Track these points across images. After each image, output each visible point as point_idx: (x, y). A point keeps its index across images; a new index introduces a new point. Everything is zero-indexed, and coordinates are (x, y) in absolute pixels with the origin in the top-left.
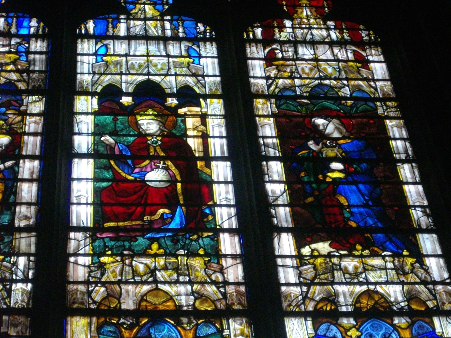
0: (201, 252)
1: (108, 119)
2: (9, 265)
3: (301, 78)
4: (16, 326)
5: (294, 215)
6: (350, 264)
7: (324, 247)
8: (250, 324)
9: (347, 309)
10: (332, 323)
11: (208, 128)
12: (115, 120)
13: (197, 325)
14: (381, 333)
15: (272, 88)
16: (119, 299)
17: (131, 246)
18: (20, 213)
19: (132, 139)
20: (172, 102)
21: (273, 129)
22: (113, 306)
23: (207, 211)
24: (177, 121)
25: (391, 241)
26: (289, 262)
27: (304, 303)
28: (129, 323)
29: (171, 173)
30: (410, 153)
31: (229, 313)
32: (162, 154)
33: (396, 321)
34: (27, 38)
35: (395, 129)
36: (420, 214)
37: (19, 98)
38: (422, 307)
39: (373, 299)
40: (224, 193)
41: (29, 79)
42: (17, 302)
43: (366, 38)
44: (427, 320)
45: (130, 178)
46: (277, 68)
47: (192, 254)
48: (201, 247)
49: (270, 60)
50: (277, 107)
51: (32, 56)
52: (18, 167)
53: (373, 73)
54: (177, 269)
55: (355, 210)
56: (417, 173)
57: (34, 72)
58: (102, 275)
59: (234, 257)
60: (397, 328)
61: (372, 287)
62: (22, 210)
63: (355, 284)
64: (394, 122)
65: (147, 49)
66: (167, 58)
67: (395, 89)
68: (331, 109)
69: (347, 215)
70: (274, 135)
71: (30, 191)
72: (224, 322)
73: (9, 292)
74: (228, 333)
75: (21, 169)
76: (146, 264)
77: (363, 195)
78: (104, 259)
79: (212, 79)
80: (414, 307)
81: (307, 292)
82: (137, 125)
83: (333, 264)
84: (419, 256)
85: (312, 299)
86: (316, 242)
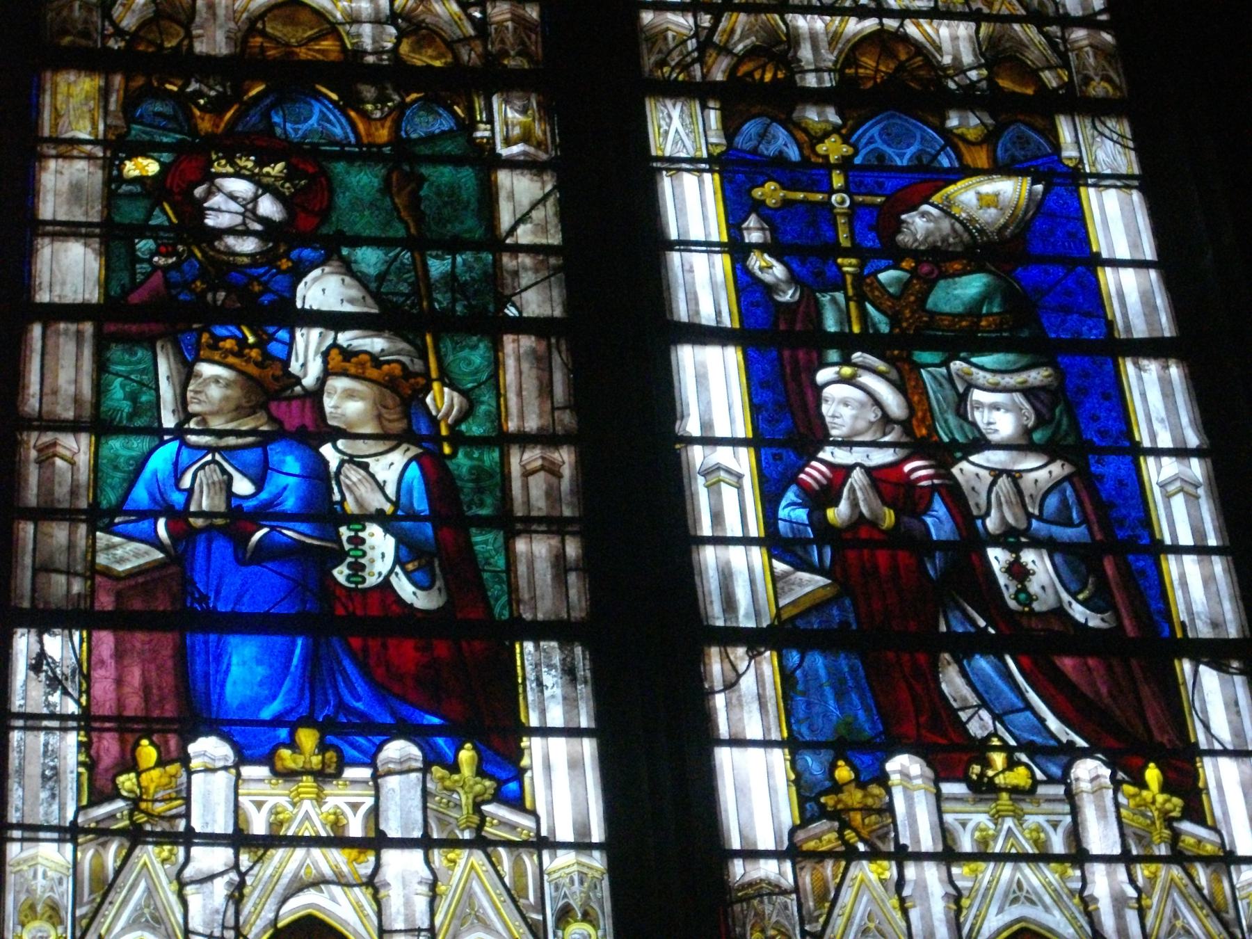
8: (546, 112)
9: (820, 80)
13: (402, 107)
27: (701, 60)
28: (213, 93)
31: (493, 78)
38: (1026, 85)
39: (894, 56)
44: (1039, 122)
60: (956, 140)
72: (478, 104)
74: (487, 134)
80: (1005, 83)
81: (713, 29)
85: (725, 50)
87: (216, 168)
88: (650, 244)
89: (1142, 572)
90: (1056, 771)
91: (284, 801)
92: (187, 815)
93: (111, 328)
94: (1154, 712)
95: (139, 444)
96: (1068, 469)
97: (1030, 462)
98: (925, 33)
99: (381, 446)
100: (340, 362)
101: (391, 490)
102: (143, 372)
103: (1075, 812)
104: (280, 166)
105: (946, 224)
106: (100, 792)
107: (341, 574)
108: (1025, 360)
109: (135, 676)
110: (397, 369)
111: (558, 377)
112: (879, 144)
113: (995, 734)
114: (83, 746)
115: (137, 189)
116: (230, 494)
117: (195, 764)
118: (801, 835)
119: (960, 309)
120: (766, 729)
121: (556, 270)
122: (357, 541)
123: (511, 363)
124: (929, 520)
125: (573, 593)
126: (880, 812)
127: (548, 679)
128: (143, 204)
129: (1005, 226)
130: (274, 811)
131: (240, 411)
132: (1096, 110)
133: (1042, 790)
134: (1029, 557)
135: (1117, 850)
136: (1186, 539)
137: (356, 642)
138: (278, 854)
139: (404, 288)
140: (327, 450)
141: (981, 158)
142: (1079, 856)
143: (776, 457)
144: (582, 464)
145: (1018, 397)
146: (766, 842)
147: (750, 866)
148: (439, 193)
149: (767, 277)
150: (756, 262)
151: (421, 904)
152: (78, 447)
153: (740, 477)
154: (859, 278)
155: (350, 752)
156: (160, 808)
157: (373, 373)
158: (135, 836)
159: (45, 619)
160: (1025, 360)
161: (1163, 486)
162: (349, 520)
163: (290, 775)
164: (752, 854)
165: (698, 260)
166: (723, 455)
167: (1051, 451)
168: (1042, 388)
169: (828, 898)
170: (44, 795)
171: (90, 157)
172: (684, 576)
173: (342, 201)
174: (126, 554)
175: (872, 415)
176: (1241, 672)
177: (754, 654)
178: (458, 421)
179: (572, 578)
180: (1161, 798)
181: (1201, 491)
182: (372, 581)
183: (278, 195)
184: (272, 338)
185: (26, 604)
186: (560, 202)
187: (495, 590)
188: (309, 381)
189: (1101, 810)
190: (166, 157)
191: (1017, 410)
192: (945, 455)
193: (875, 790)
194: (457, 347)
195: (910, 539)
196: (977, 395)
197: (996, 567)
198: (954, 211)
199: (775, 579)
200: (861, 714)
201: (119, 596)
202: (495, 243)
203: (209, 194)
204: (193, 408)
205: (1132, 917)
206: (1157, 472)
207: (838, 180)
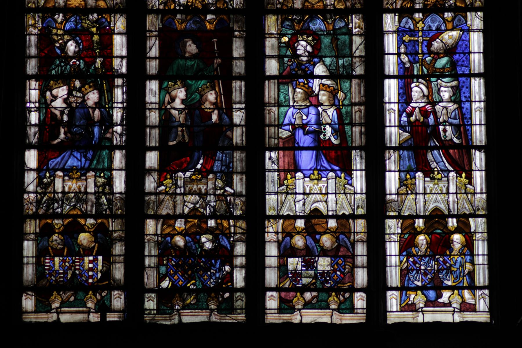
4: (237, 22)
9: (419, 6)
13: (335, 20)
14: (436, 25)
22: (289, 6)
33: (446, 15)
38: (462, 4)
44: (464, 14)
72: (350, 17)
80: (458, 4)
87: (299, 39)
89: (468, 130)
90: (446, 175)
91: (312, 185)
92: (296, 188)
93: (280, 81)
94: (466, 162)
95: (286, 108)
96: (457, 106)
97: (450, 104)
99: (329, 107)
100: (322, 86)
101: (331, 117)
102: (286, 91)
103: (448, 184)
104: (311, 37)
105: (441, 44)
106: (281, 185)
107: (322, 136)
108: (453, 79)
109: (286, 161)
110: (332, 88)
111: (362, 89)
113: (436, 167)
114: (278, 175)
115: (284, 45)
116: (302, 119)
117: (297, 178)
118: (399, 190)
119: (441, 67)
120: (395, 168)
121: (364, 62)
122: (325, 129)
123: (353, 86)
124: (429, 119)
125: (363, 139)
126: (414, 184)
127: (357, 159)
128: (285, 49)
130: (310, 187)
131: (304, 100)
132: (476, 10)
133: (443, 179)
134: (447, 127)
135: (455, 192)
136: (478, 123)
137: (324, 151)
138: (311, 196)
139: (334, 68)
140: (319, 108)
141: (450, 26)
142: (448, 193)
143: (402, 106)
144: (366, 110)
145: (450, 89)
146: (393, 192)
147: (390, 196)
148: (341, 43)
149: (404, 61)
150: (402, 56)
151: (334, 205)
152: (275, 109)
153: (395, 111)
154: (422, 59)
155: (323, 175)
156: (291, 187)
157: (328, 89)
158: (287, 193)
159: (271, 149)
160: (453, 79)
161: (475, 109)
162: (323, 124)
163: (312, 180)
164: (390, 194)
166: (392, 106)
167: (454, 102)
168: (455, 86)
169: (403, 202)
170: (272, 185)
171: (275, 37)
172: (383, 133)
173: (323, 46)
174: (284, 134)
175: (421, 95)
176: (484, 152)
177: (394, 152)
178: (343, 100)
179: (363, 136)
180: (464, 180)
181: (482, 110)
182: (327, 138)
183: (311, 45)
184: (310, 82)
185: (267, 146)
186: (365, 44)
187: (349, 139)
188: (316, 92)
189: (453, 183)
190: (289, 36)
191: (449, 92)
192: (433, 104)
193: (413, 180)
194: (344, 82)
195: (425, 124)
196: (442, 89)
197: (441, 130)
198: (443, 41)
199: (399, 134)
200: (412, 164)
201: (284, 143)
202: (352, 56)
203: (298, 45)
204: (296, 99)
205: (456, 205)
206: (475, 105)
207: (420, 34)
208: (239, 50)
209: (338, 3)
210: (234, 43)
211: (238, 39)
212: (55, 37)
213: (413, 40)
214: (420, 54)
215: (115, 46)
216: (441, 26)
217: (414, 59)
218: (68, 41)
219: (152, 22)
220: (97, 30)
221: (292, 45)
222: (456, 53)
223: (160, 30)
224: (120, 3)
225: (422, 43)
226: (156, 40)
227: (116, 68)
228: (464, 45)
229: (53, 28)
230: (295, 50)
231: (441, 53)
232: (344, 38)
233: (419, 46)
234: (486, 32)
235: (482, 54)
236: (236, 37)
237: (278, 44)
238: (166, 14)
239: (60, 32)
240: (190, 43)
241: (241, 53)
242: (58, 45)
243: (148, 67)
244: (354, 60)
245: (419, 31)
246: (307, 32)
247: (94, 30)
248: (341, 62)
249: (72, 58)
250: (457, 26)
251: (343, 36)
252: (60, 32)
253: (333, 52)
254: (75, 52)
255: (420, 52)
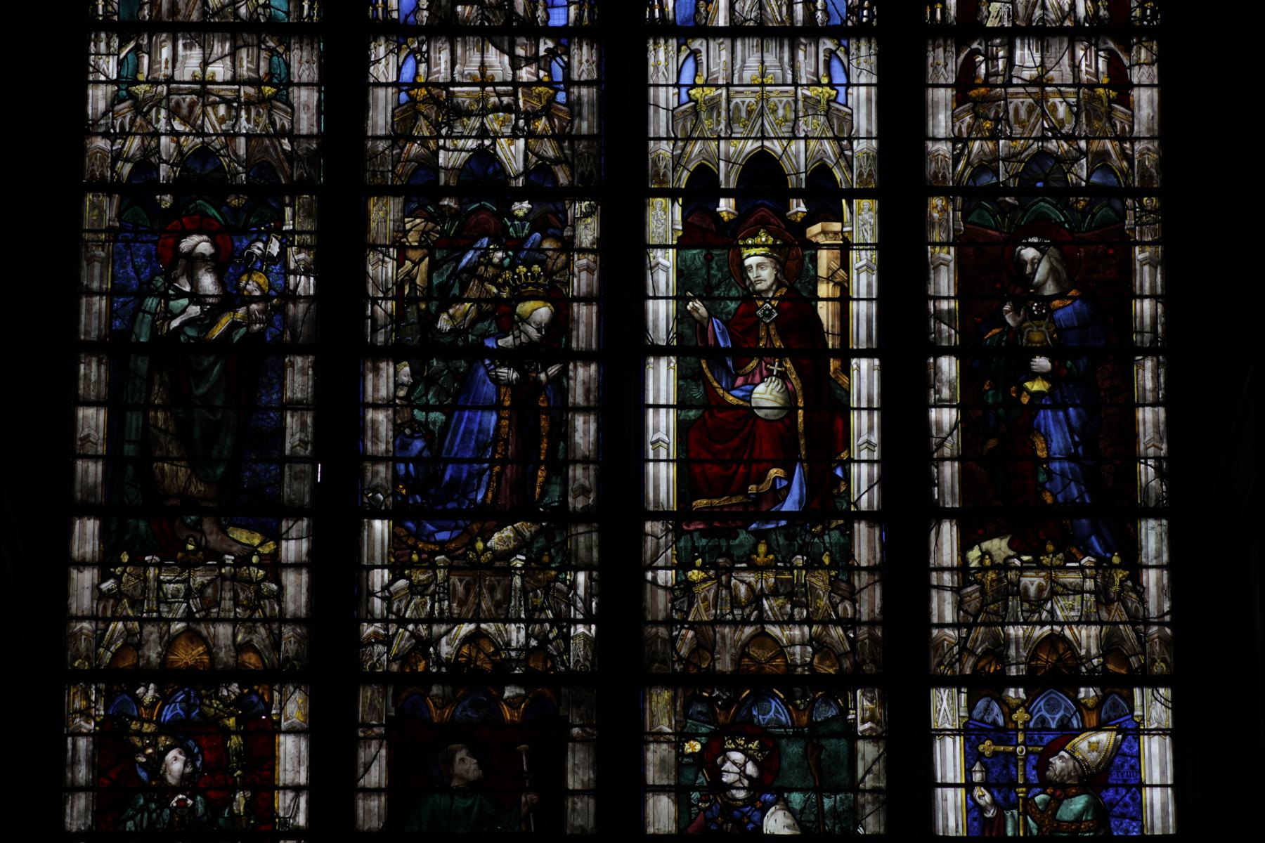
0: (826, 560)
1: (696, 254)
2: (565, 588)
3: (1010, 138)
5: (965, 476)
6: (1032, 582)
7: (998, 547)
8: (883, 701)
9: (1018, 670)
10: (993, 698)
11: (851, 288)
12: (708, 259)
13: (814, 701)
14: (1058, 716)
15: (960, 167)
16: (712, 652)
17: (729, 546)
18: (575, 479)
19: (733, 305)
20: (798, 208)
21: (952, 276)
22: (704, 666)
23: (839, 472)
24: (804, 256)
25: (1100, 538)
26: (947, 577)
27: (959, 660)
29: (790, 386)
30: (1160, 329)
32: (778, 344)
34: (565, 37)
35: (1146, 268)
36: (1151, 470)
37: (559, 206)
38: (1121, 667)
39: (1056, 651)
40: (864, 428)
41: (573, 156)
42: (578, 661)
43: (1137, 13)
44: (1125, 692)
45: (730, 398)
46: (973, 109)
47: (813, 565)
48: (826, 549)
49: (964, 84)
50: (964, 218)
51: (575, 90)
52: (568, 378)
53: (1133, 116)
54: (790, 596)
55: (1056, 466)
56: (1162, 380)
57: (581, 137)
58: (691, 605)
59: (869, 569)
61: (1057, 628)
62: (578, 473)
63: (1034, 624)
64: (1148, 252)
65: (763, 63)
66: (792, 88)
67: (1163, 164)
68: (1048, 219)
69: (1042, 478)
70: (952, 294)
71: (586, 433)
72: (850, 696)
73: (567, 638)
75: (571, 382)
76: (749, 585)
77: (1072, 431)
78: (695, 575)
79: (863, 143)
80: (1110, 667)
81: (967, 639)
82: (744, 270)
83: (1010, 582)
84: (1135, 568)
85: (972, 652)
86: (990, 538)
88: (927, 783)
98: (1074, 634)
105: (1071, 763)
112: (1044, 713)
115: (690, 760)
128: (693, 770)
129: (1100, 763)
139: (812, 818)
141: (1092, 720)
149: (982, 802)
150: (978, 792)
154: (1025, 799)
165: (950, 792)
171: (669, 742)
173: (785, 764)
183: (756, 763)
186: (887, 761)
190: (703, 739)
198: (1076, 754)
202: (854, 786)
203: (724, 762)
207: (1021, 738)
208: (581, 772)
209: (821, 661)
210: (569, 753)
211: (578, 746)
212: (137, 741)
213: (1004, 752)
214: (1021, 786)
215: (282, 762)
216: (1070, 719)
217: (1006, 798)
218: (168, 749)
219: (371, 703)
220: (237, 722)
221: (710, 761)
222: (1108, 786)
223: (391, 724)
224: (296, 658)
225: (1026, 760)
226: (380, 746)
227: (281, 814)
228: (1126, 766)
229: (132, 718)
230: (717, 772)
231: (1071, 786)
232: (836, 745)
233: (1017, 767)
234: (1179, 735)
235: (1170, 790)
236: (574, 740)
237: (677, 758)
238: (407, 681)
239: (147, 728)
240: (462, 754)
241: (586, 779)
242: (142, 759)
243: (361, 812)
244: (861, 799)
245: (1017, 730)
246: (744, 729)
247: (231, 722)
248: (827, 803)
249: (175, 790)
250: (1110, 719)
251: (834, 741)
252: (147, 728)
253: (810, 778)
254: (183, 776)
255: (1021, 781)
